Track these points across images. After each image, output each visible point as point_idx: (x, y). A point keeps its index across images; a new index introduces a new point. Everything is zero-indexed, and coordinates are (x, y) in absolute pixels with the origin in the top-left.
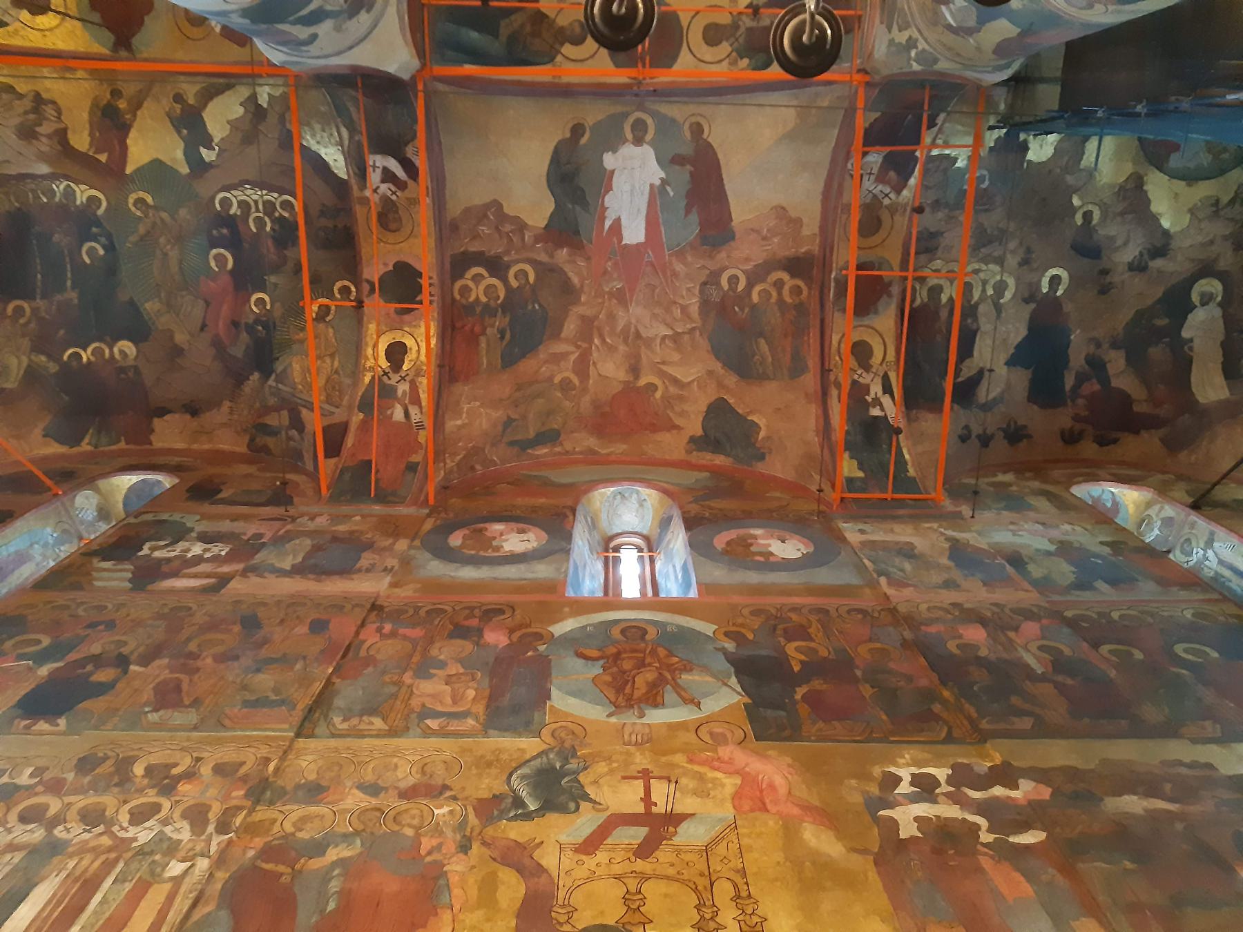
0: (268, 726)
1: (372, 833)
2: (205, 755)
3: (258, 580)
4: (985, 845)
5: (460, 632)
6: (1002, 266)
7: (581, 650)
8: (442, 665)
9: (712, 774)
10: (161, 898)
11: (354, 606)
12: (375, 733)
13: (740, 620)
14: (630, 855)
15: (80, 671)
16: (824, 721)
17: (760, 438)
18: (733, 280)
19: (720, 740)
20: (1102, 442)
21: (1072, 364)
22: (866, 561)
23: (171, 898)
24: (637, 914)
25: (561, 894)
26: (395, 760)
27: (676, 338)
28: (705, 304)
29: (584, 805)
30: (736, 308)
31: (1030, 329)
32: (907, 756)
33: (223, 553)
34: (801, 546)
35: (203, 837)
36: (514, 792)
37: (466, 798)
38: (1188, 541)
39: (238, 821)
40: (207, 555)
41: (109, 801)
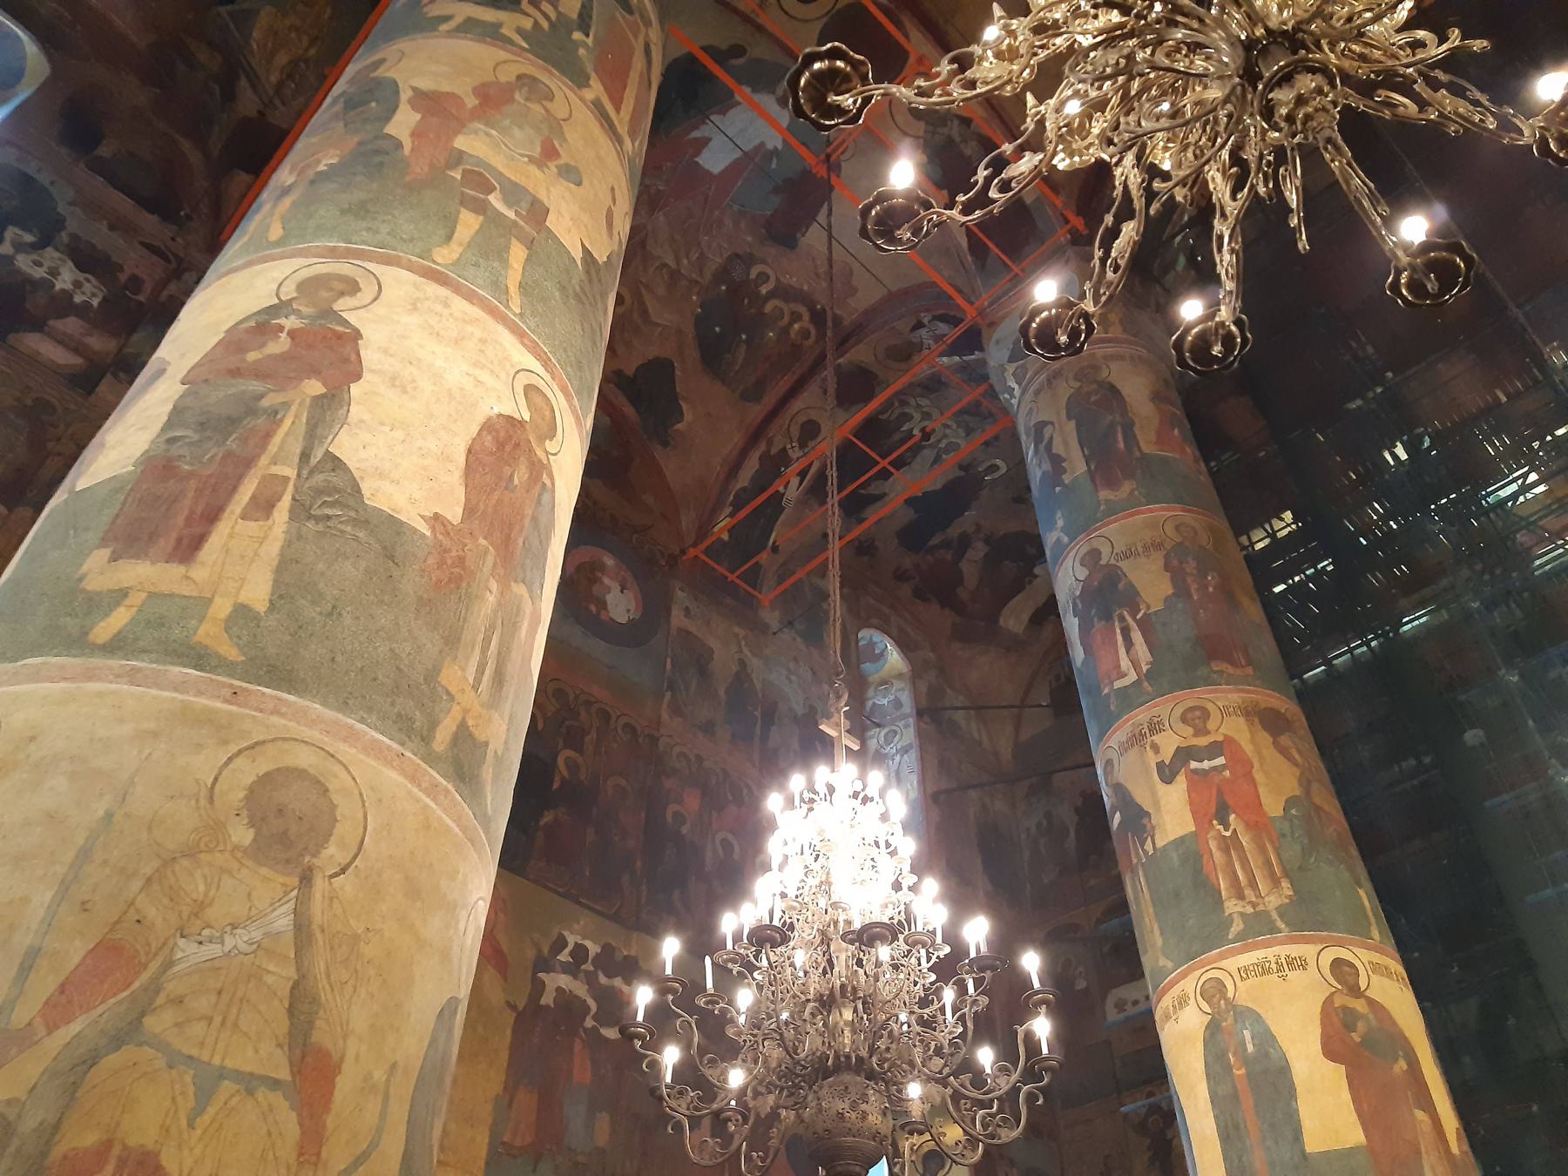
4: (585, 1030)
6: (967, 435)
17: (676, 427)
18: (764, 277)
20: (918, 594)
21: (949, 530)
22: (669, 660)
27: (675, 275)
28: (723, 274)
30: (746, 301)
31: (944, 487)
32: (582, 923)
33: (95, 302)
34: (632, 606)
38: (895, 732)
40: (78, 299)
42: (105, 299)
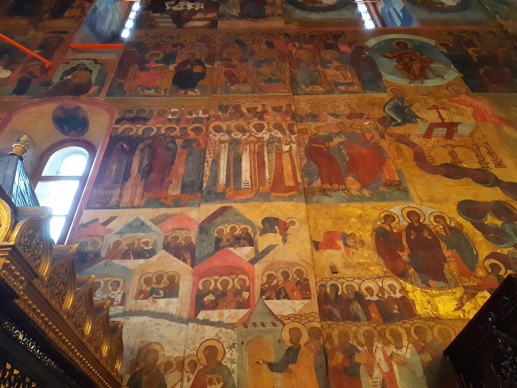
0: (281, 91)
1: (346, 133)
2: (265, 103)
3: (229, 22)
5: (328, 47)
7: (384, 54)
8: (331, 62)
9: (461, 107)
10: (288, 158)
11: (279, 34)
12: (322, 92)
13: (444, 38)
14: (444, 138)
15: (186, 68)
16: (495, 84)
19: (458, 93)
23: (291, 157)
24: (457, 159)
25: (426, 153)
26: (337, 104)
29: (418, 120)
33: (202, 7)
35: (287, 136)
36: (389, 115)
37: (373, 118)
39: (295, 129)
41: (242, 122)
42: (204, 5)
